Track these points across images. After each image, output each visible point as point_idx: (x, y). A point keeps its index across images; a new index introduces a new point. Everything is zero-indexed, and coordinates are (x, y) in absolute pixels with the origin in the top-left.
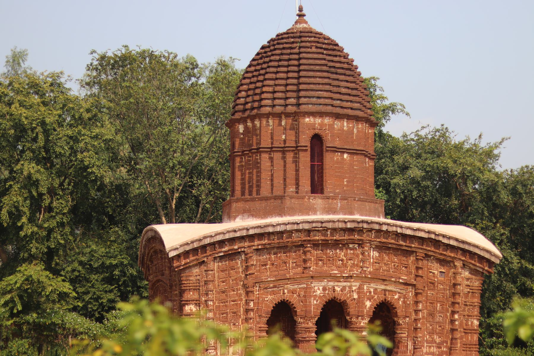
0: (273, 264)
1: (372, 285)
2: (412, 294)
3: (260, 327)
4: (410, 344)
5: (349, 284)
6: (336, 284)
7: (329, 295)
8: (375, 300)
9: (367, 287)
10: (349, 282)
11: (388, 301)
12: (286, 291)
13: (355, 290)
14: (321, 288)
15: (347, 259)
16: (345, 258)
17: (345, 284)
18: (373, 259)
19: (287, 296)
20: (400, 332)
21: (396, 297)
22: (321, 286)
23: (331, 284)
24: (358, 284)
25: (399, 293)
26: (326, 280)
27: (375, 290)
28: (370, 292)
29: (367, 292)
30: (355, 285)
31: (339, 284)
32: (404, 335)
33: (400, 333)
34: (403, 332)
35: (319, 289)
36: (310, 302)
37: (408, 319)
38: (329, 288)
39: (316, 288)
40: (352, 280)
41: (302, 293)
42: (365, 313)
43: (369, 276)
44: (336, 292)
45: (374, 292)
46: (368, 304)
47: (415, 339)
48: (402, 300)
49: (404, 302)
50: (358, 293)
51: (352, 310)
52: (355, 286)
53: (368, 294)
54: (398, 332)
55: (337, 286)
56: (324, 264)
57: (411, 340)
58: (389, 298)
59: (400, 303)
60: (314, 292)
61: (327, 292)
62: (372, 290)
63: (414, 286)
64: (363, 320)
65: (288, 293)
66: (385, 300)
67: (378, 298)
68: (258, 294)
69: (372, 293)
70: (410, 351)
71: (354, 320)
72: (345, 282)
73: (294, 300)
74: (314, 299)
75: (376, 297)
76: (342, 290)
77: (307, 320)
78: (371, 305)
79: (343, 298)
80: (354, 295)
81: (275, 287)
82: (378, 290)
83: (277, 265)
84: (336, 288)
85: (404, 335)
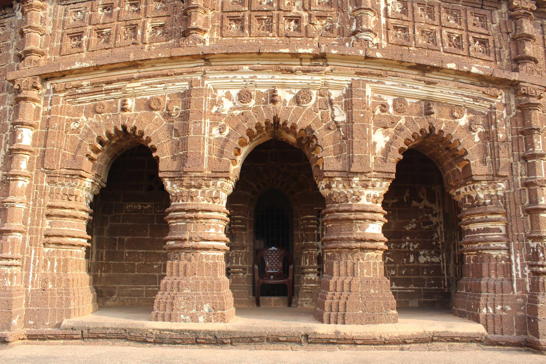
0: (100, 32)
1: (389, 83)
2: (508, 114)
3: (50, 207)
4: (517, 260)
5: (318, 79)
6: (279, 78)
7: (258, 113)
8: (401, 129)
9: (374, 91)
10: (319, 72)
11: (441, 131)
12: (131, 103)
13: (339, 98)
14: (234, 93)
15: (310, 16)
16: (305, 14)
17: (307, 78)
18: (387, 17)
19: (133, 117)
20: (481, 226)
21: (463, 121)
22: (236, 87)
23: (265, 80)
24: (345, 80)
25: (470, 111)
26: (246, 68)
27: (399, 102)
28: (384, 107)
29: (374, 105)
30: (338, 81)
31: (289, 79)
32: (496, 235)
33: (479, 231)
34: (489, 225)
35: (228, 96)
36: (198, 131)
37: (503, 185)
38: (259, 94)
39: (221, 93)
40: (328, 69)
41: (177, 108)
42: (372, 166)
43: (378, 55)
44: (278, 105)
45: (394, 106)
46: (380, 139)
47: (534, 245)
48: (480, 129)
49: (488, 136)
50: (348, 107)
51: (328, 159)
52: (338, 87)
53: (378, 111)
54: (473, 227)
55: (283, 86)
56: (242, 28)
57: (518, 249)
58: (441, 122)
59: (477, 139)
60: (213, 103)
61: (252, 103)
62: (390, 101)
63: (513, 86)
64: (366, 187)
65: (138, 108)
66: (432, 129)
67: (411, 125)
68: (49, 113)
69: (391, 110)
70: (521, 284)
71: (338, 187)
72: (306, 72)
73: (156, 132)
74: (213, 124)
75: (402, 121)
76: (297, 100)
77: (190, 186)
78: (389, 145)
79: (301, 123)
80: (336, 112)
81: (96, 88)
82: (408, 100)
83: (109, 34)
84: (280, 93)
85: (496, 235)
